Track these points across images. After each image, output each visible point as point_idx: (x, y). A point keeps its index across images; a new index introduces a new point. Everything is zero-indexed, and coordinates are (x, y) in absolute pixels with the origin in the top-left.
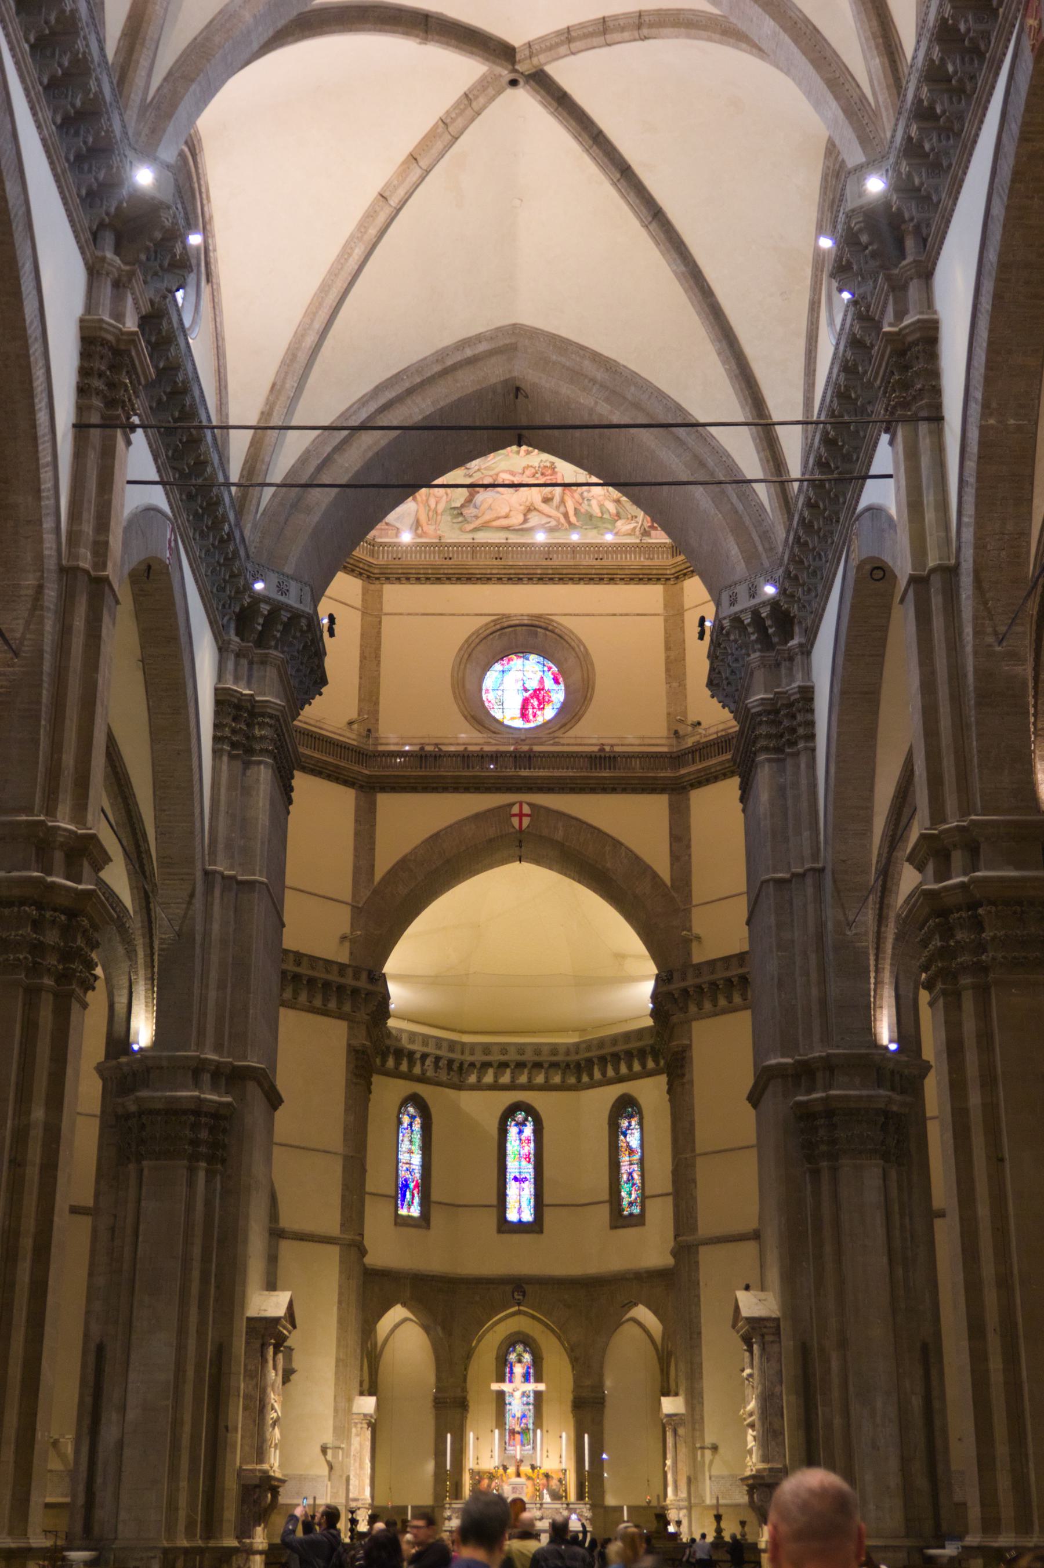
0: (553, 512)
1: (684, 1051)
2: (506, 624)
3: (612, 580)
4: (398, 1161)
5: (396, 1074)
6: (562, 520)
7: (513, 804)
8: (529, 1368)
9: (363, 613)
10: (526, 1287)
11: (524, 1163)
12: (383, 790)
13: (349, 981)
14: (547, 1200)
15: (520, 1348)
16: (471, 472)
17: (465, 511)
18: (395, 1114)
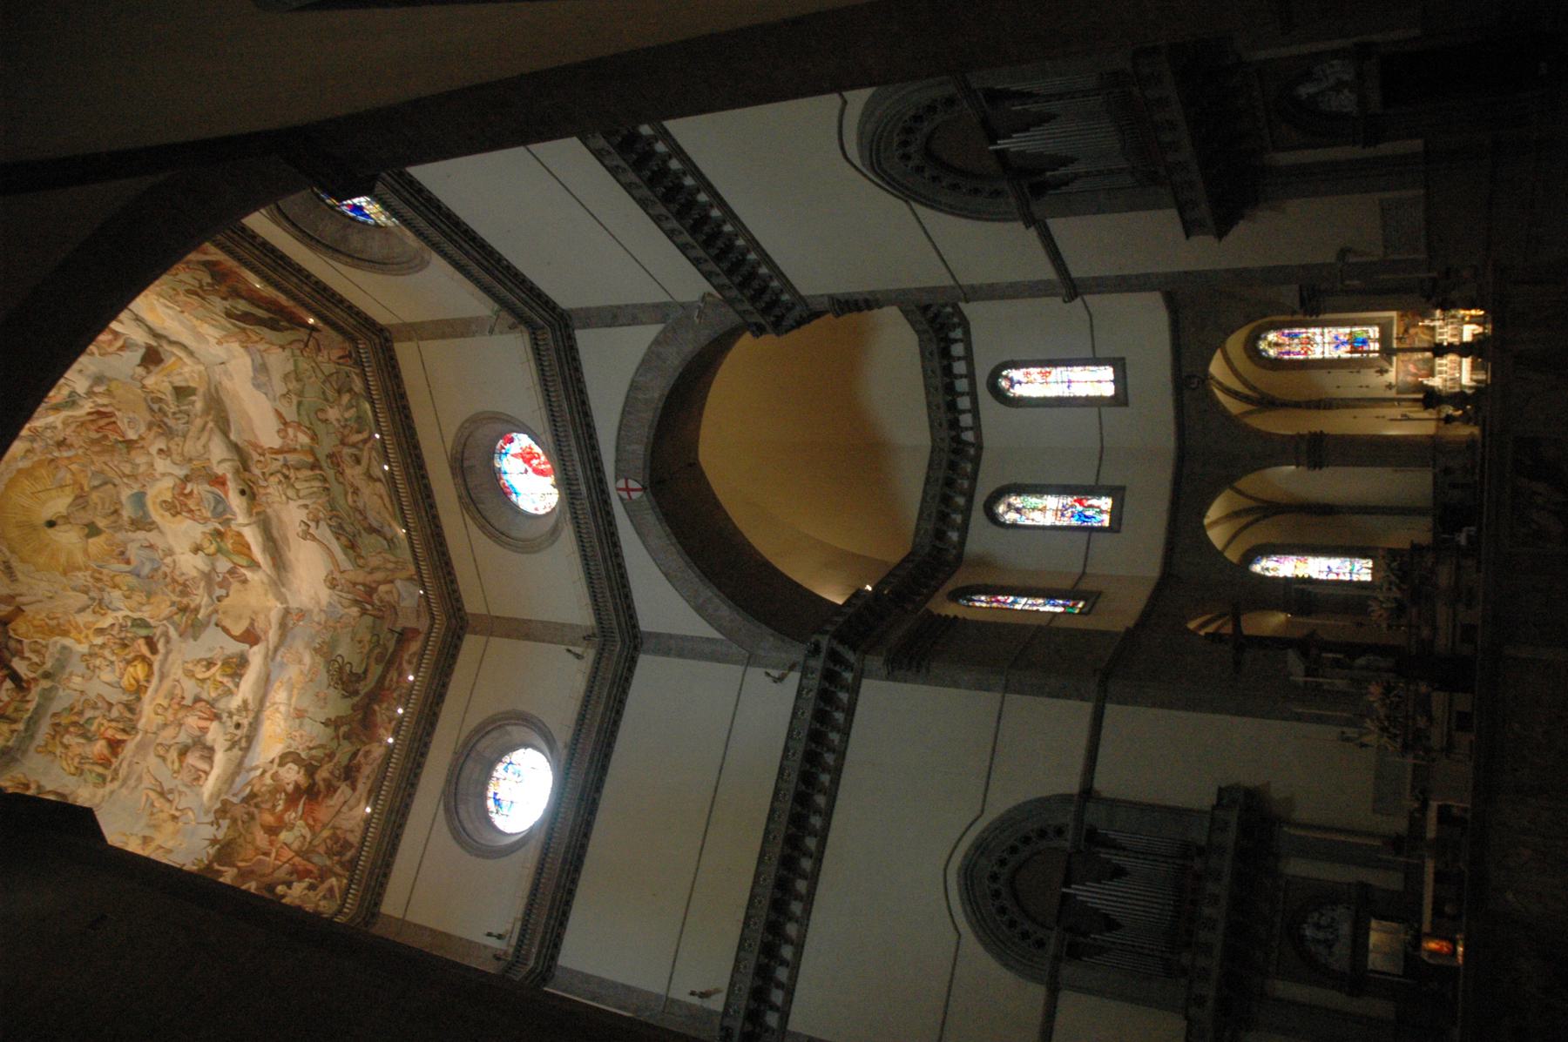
0: (366, 454)
1: (839, 301)
2: (468, 500)
3: (403, 396)
4: (1054, 528)
5: (964, 529)
6: (369, 445)
7: (622, 499)
8: (1283, 334)
9: (491, 635)
10: (1184, 374)
11: (1051, 378)
12: (635, 626)
13: (814, 681)
14: (1089, 354)
15: (1262, 345)
16: (356, 532)
17: (389, 536)
18: (1002, 531)
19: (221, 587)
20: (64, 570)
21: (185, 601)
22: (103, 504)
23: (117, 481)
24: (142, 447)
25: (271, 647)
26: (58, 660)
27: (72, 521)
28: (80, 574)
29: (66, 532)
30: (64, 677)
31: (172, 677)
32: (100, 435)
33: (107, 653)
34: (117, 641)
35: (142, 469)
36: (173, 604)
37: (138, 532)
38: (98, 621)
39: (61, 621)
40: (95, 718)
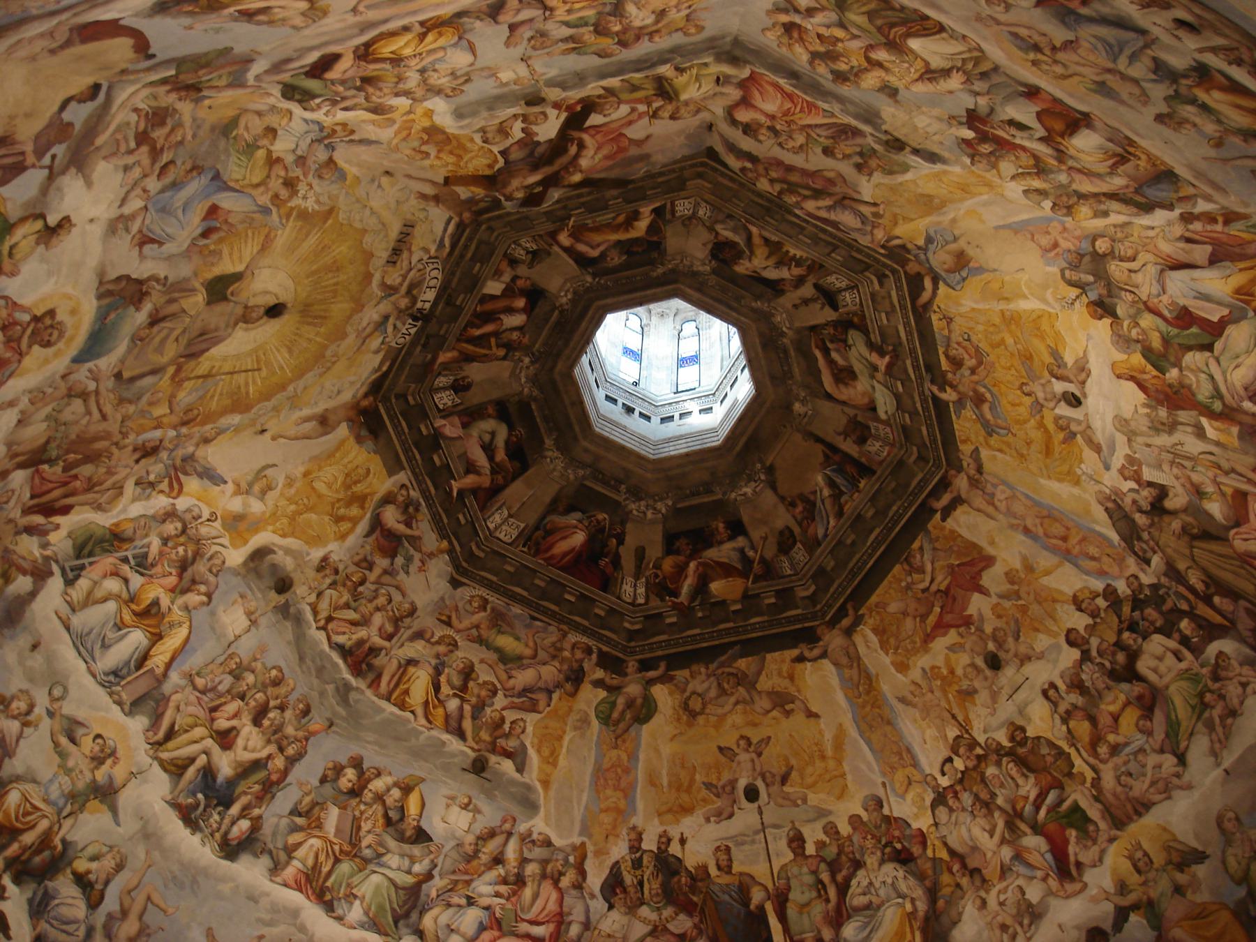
19: (70, 125)
20: (325, 222)
21: (168, 99)
22: (167, 337)
23: (110, 383)
24: (16, 455)
25: (64, 16)
26: (490, 109)
27: (239, 310)
28: (310, 204)
29: (266, 292)
30: (517, 87)
31: (352, 19)
32: (74, 472)
33: (412, 80)
34: (370, 90)
35: (48, 409)
36: (197, 101)
37: (145, 276)
38: (364, 121)
39: (416, 144)
40: (567, 24)
